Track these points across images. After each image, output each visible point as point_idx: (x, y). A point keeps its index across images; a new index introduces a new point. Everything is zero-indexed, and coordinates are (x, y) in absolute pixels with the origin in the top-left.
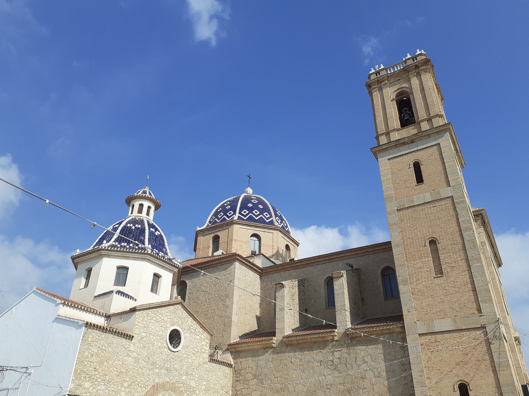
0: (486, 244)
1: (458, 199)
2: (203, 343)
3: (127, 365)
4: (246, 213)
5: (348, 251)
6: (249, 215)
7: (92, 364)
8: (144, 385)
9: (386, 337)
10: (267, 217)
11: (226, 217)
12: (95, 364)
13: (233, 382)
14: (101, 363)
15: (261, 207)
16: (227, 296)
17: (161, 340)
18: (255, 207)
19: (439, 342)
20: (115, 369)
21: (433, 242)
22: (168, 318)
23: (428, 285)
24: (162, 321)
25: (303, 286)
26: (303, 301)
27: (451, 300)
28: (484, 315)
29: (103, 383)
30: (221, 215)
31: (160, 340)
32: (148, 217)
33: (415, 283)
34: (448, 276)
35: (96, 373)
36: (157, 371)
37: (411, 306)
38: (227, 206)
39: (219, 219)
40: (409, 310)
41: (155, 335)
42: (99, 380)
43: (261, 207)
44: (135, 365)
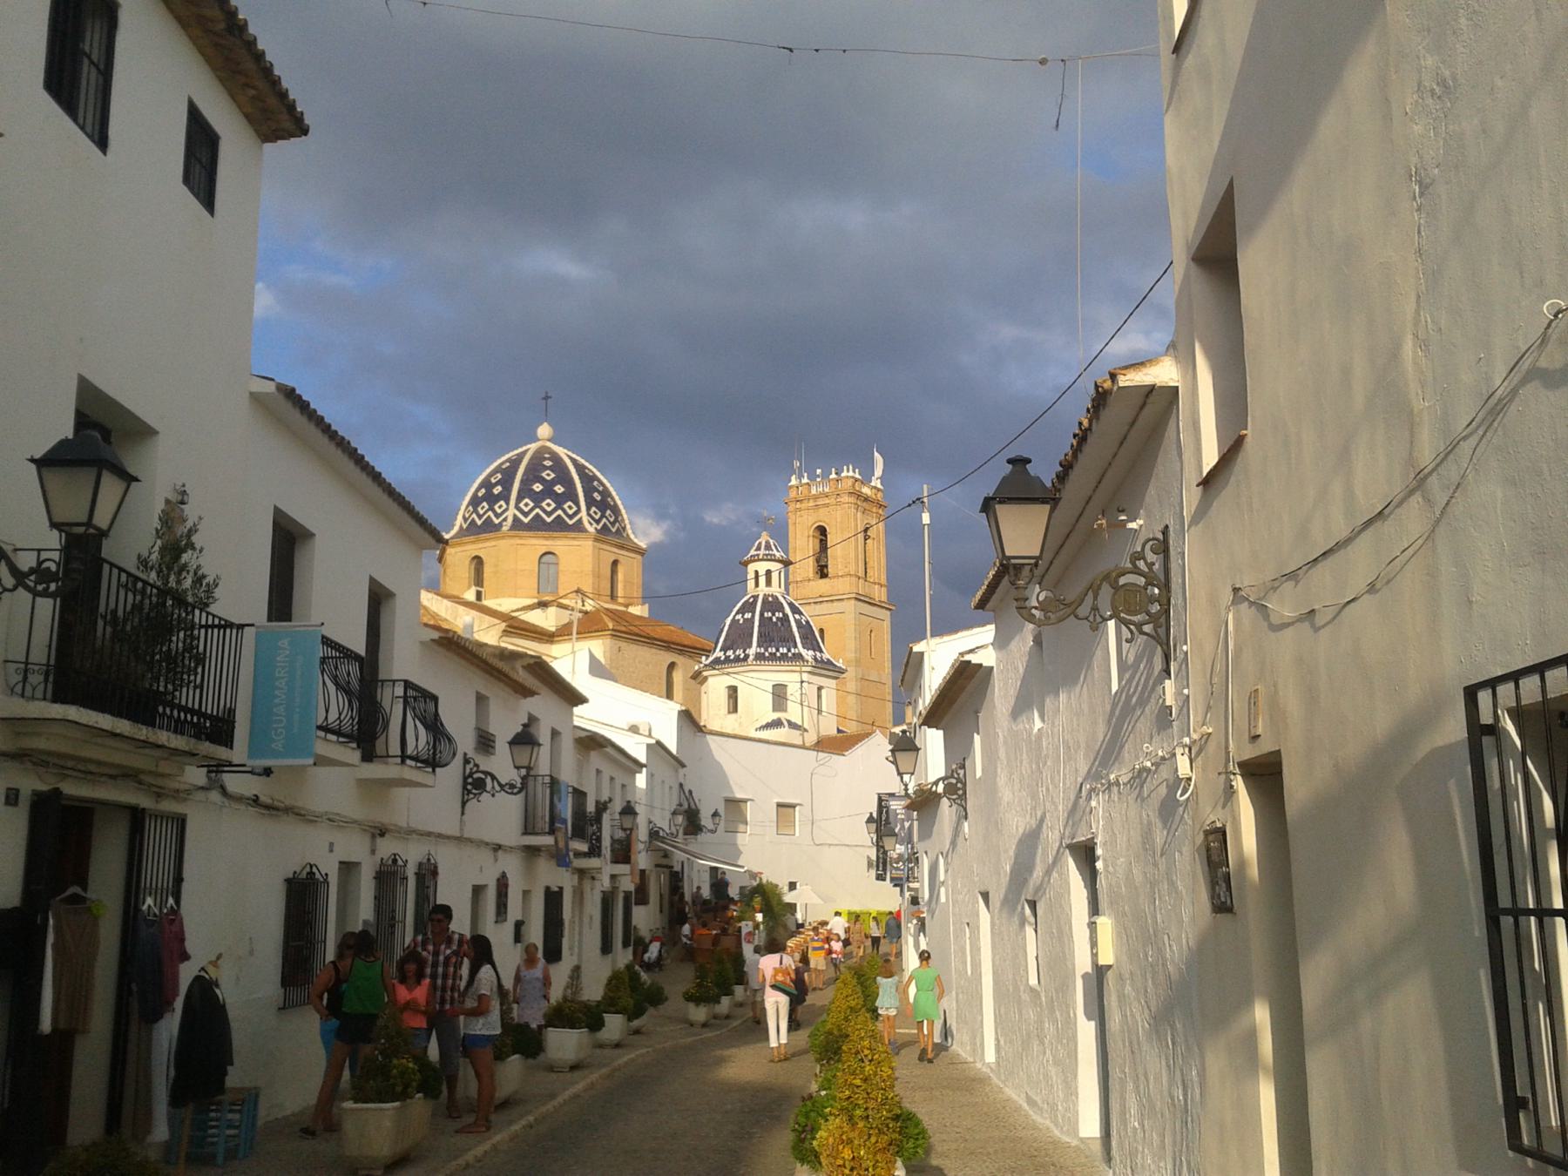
4: (529, 507)
10: (570, 512)
15: (559, 489)
30: (483, 507)
39: (480, 517)
43: (559, 489)
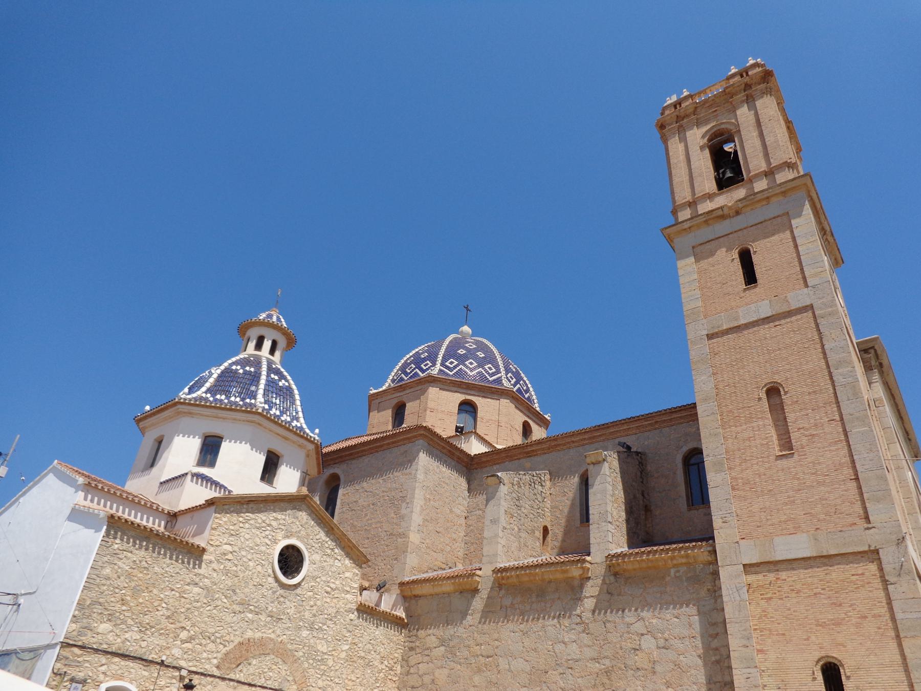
0: (883, 403)
1: (821, 309)
2: (347, 574)
3: (188, 601)
4: (453, 365)
5: (623, 422)
6: (458, 368)
7: (117, 591)
8: (222, 640)
9: (681, 571)
11: (418, 371)
12: (123, 592)
13: (404, 651)
14: (136, 592)
15: (481, 355)
16: (403, 498)
17: (263, 560)
18: (471, 354)
19: (783, 580)
20: (164, 605)
21: (773, 392)
22: (280, 524)
23: (762, 470)
24: (268, 528)
25: (542, 485)
26: (540, 511)
27: (808, 498)
28: (874, 527)
29: (136, 629)
31: (261, 561)
32: (271, 357)
33: (738, 469)
34: (803, 453)
35: (124, 608)
36: (250, 616)
37: (729, 512)
38: (422, 353)
39: (406, 374)
40: (726, 519)
41: (252, 551)
42: (130, 622)
43: (481, 355)
44: (205, 601)
